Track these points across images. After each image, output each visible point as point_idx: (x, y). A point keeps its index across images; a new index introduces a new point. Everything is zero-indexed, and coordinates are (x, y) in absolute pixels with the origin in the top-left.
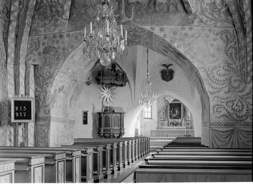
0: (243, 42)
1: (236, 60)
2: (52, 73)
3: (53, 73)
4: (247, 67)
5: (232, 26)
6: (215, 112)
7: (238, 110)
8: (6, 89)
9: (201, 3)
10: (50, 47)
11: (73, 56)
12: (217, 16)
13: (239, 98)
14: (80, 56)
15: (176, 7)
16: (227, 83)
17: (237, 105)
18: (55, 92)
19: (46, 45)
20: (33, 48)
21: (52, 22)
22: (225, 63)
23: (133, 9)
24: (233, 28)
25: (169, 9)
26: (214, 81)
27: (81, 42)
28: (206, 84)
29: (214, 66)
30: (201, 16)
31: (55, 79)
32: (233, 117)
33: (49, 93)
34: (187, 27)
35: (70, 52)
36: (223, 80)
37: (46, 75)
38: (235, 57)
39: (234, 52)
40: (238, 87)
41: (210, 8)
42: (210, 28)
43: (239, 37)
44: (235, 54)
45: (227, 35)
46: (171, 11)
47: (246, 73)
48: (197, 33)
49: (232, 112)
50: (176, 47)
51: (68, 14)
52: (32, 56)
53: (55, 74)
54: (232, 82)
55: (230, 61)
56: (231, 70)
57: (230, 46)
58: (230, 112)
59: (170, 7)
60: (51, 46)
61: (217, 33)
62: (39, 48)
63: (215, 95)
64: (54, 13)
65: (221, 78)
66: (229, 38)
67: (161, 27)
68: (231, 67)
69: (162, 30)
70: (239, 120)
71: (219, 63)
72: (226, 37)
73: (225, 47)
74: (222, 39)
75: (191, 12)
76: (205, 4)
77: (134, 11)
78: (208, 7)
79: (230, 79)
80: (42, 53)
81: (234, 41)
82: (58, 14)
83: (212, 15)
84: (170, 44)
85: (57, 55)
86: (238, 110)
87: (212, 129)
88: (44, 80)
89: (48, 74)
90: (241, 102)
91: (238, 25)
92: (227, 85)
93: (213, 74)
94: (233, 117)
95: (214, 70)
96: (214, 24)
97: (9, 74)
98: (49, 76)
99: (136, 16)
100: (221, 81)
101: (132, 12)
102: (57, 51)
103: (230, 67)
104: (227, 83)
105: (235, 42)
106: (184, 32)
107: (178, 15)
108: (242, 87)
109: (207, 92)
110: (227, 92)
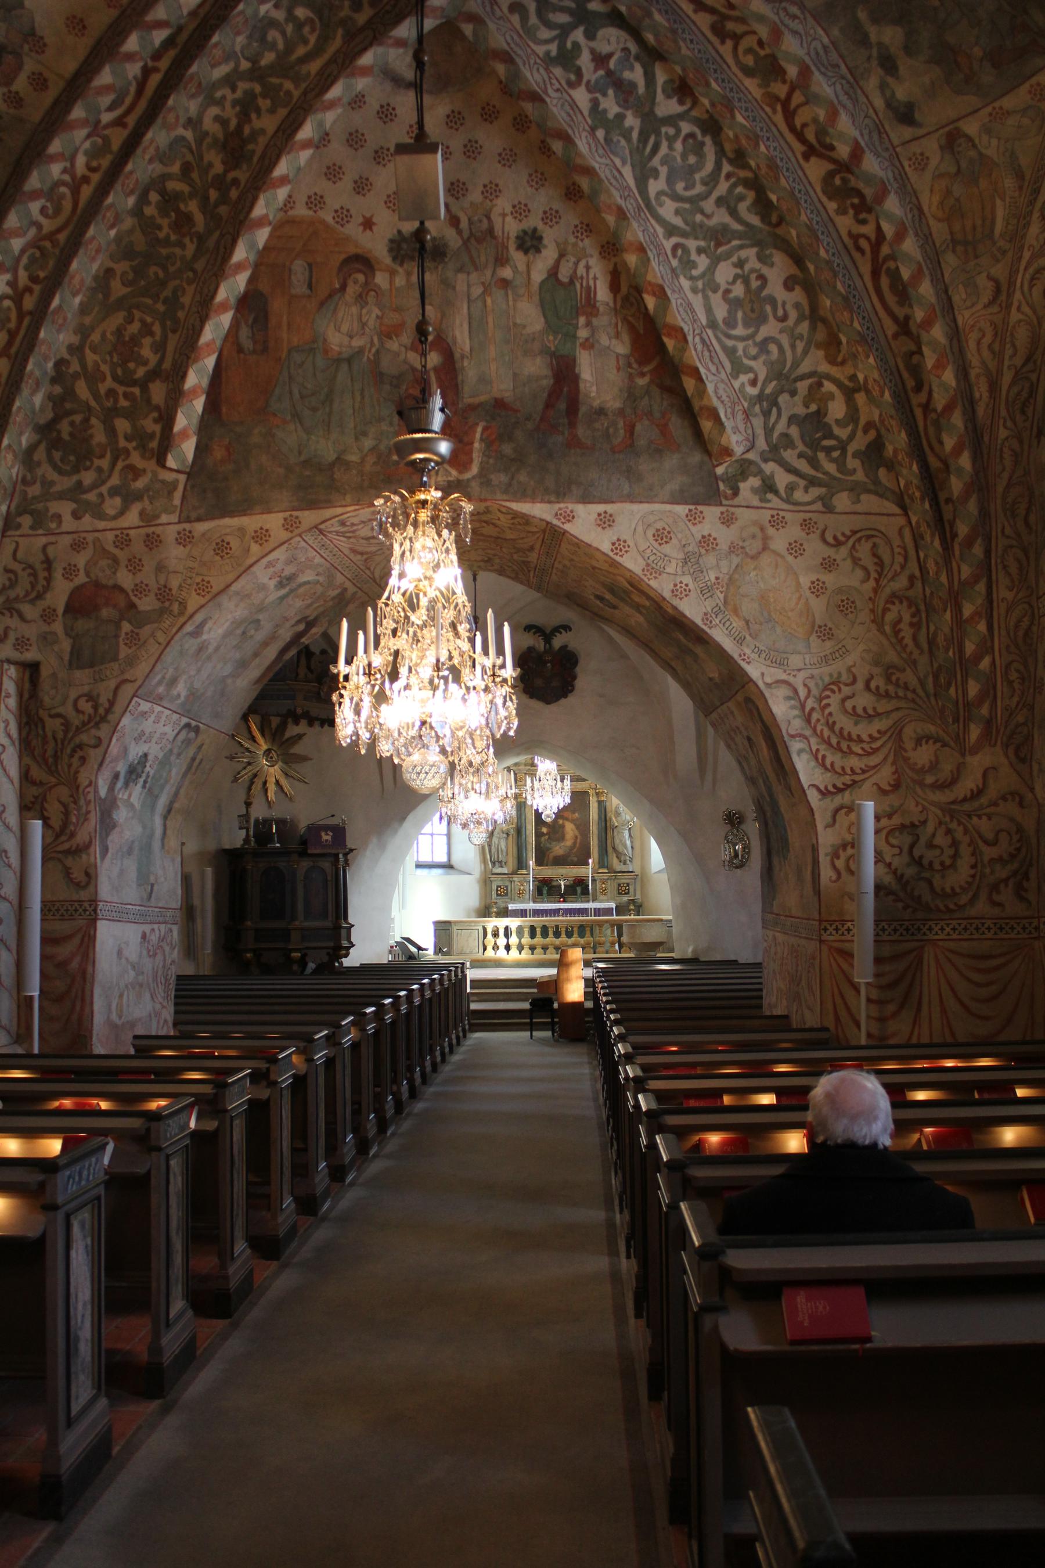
0: (944, 578)
1: (916, 652)
2: (103, 700)
3: (112, 703)
4: (965, 682)
5: (897, 510)
7: (937, 866)
9: (766, 414)
11: (202, 625)
12: (831, 468)
13: (939, 812)
15: (664, 429)
16: (885, 750)
17: (931, 846)
18: (111, 788)
19: (81, 579)
20: (19, 591)
21: (115, 480)
22: (876, 663)
23: (479, 429)
24: (901, 521)
25: (632, 434)
26: (834, 741)
27: (242, 569)
29: (831, 675)
30: (769, 467)
31: (119, 728)
32: (916, 893)
33: (91, 789)
34: (712, 512)
35: (190, 609)
36: (870, 736)
37: (78, 711)
38: (915, 639)
39: (907, 618)
40: (934, 766)
41: (802, 437)
42: (808, 516)
43: (926, 556)
44: (912, 625)
45: (875, 545)
46: (642, 442)
47: (961, 706)
48: (754, 537)
49: (911, 872)
50: (667, 595)
51: (188, 448)
52: (14, 622)
53: (118, 708)
54: (909, 745)
55: (892, 657)
56: (901, 693)
57: (894, 595)
58: (902, 875)
59: (638, 428)
60: (104, 582)
61: (835, 538)
62: (45, 592)
63: (838, 800)
64: (122, 443)
65: (861, 726)
66: (886, 558)
67: (601, 508)
68: (898, 679)
69: (605, 521)
70: (942, 908)
71: (851, 663)
72: (875, 555)
73: (870, 599)
74: (856, 561)
75: (727, 452)
76: (784, 420)
77: (482, 440)
78: (794, 431)
79: (896, 733)
80: (60, 610)
81: (907, 572)
82: (142, 447)
83: (814, 463)
85: (130, 623)
87: (830, 948)
90: (949, 832)
92: (885, 759)
93: (827, 711)
94: (916, 893)
95: (828, 693)
96: (820, 498)
98: (90, 715)
99: (491, 461)
100: (860, 740)
101: (476, 445)
102: (132, 606)
103: (894, 678)
104: (885, 750)
105: (912, 578)
107: (671, 461)
108: (947, 768)
109: (806, 786)
110: (888, 788)
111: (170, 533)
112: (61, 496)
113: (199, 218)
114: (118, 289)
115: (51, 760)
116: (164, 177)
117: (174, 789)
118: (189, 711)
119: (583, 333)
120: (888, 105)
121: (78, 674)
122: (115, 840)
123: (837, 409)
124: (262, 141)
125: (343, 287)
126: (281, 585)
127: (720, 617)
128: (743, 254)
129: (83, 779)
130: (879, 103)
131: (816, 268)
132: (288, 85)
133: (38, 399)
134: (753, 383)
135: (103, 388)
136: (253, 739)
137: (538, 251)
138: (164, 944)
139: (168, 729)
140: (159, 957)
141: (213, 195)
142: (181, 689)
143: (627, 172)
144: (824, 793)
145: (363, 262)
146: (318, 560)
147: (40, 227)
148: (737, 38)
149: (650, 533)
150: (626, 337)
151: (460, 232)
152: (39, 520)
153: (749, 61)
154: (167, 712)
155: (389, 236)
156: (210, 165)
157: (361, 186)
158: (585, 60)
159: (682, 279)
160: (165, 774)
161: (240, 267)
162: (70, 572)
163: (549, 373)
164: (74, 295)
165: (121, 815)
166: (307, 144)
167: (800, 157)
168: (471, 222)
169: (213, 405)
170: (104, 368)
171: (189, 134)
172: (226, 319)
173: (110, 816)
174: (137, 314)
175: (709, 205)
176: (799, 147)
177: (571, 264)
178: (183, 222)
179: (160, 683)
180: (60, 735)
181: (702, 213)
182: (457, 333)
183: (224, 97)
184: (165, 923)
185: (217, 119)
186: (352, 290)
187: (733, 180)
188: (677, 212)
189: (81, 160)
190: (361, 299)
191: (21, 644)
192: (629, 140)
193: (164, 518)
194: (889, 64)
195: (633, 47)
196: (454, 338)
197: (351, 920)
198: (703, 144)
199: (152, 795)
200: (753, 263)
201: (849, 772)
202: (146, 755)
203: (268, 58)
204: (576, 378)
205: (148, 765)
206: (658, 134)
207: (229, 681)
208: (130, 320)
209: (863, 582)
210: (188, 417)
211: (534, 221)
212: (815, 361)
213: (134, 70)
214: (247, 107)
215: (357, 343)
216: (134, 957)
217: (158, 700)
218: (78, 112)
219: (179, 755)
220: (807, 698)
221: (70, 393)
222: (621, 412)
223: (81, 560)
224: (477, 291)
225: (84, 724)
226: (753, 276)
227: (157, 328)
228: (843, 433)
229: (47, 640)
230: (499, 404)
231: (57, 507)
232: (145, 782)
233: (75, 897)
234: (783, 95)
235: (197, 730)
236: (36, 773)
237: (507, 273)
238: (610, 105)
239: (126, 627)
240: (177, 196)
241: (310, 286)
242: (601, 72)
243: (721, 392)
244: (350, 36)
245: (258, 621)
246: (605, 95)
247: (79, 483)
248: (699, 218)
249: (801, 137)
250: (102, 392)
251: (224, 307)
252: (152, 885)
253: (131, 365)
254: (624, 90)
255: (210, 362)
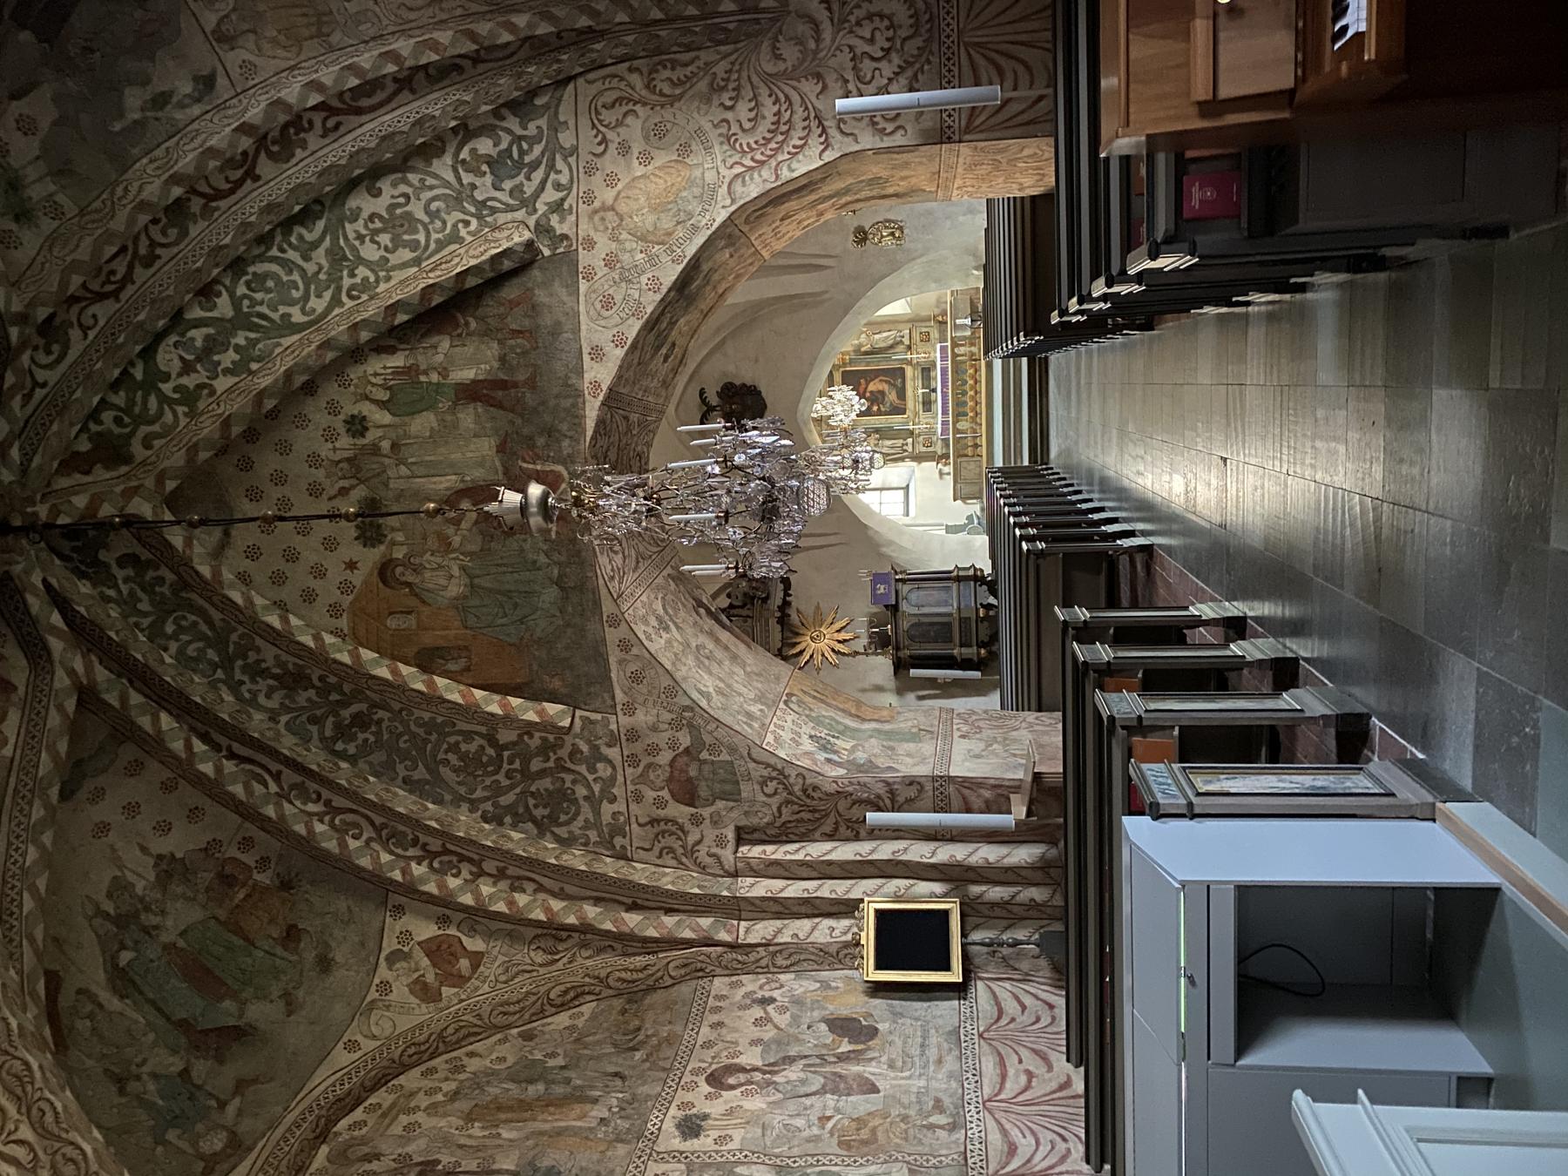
0: (630, 39)
1: (697, 63)
3: (768, 765)
5: (571, 86)
6: (899, 127)
7: (890, 34)
8: (833, 950)
9: (494, 211)
10: (670, 780)
12: (537, 150)
13: (841, 34)
15: (513, 304)
16: (787, 89)
17: (872, 41)
18: (839, 765)
19: (665, 794)
20: (677, 845)
21: (583, 769)
22: (709, 101)
23: (525, 465)
24: (581, 81)
25: (520, 332)
26: (780, 138)
27: (653, 661)
28: (793, 171)
29: (722, 143)
30: (541, 208)
32: (916, 52)
34: (584, 258)
35: (688, 702)
36: (774, 104)
37: (775, 793)
38: (686, 65)
39: (666, 73)
40: (800, 42)
41: (513, 177)
42: (581, 170)
43: (610, 57)
44: (673, 69)
45: (603, 106)
46: (527, 323)
47: (746, 17)
48: (603, 219)
49: (896, 59)
50: (658, 297)
51: (552, 708)
53: (772, 761)
54: (781, 66)
55: (702, 85)
56: (735, 76)
57: (647, 87)
58: (899, 67)
59: (514, 326)
61: (600, 144)
62: (677, 823)
63: (833, 132)
64: (551, 764)
66: (614, 95)
67: (586, 358)
68: (723, 80)
69: (598, 354)
70: (928, 26)
72: (613, 106)
74: (619, 123)
75: (530, 245)
76: (498, 194)
78: (508, 185)
79: (770, 79)
81: (626, 75)
82: (554, 747)
83: (534, 166)
84: (648, 321)
86: (890, 34)
88: (793, 803)
89: (772, 786)
90: (858, 24)
91: (567, 60)
92: (794, 88)
93: (754, 146)
94: (916, 52)
95: (737, 145)
96: (565, 159)
97: (775, 936)
100: (778, 113)
101: (539, 467)
102: (687, 750)
103: (722, 84)
104: (787, 89)
105: (630, 70)
106: (601, 271)
107: (541, 296)
109: (821, 163)
110: (820, 85)
111: (624, 720)
112: (597, 813)
113: (355, 708)
114: (420, 773)
115: (817, 815)
116: (322, 739)
118: (774, 702)
119: (435, 377)
120: (198, 100)
121: (744, 795)
122: (882, 762)
123: (485, 146)
124: (285, 657)
125: (409, 585)
126: (667, 629)
127: (675, 248)
128: (351, 235)
129: (832, 788)
130: (196, 110)
131: (357, 167)
132: (234, 637)
133: (516, 835)
134: (467, 223)
135: (505, 782)
136: (801, 652)
137: (364, 418)
138: (970, 720)
139: (789, 719)
140: (981, 724)
141: (334, 697)
142: (755, 709)
143: (286, 341)
144: (827, 145)
145: (385, 571)
146: (644, 598)
147: (370, 840)
148: (153, 244)
149: (607, 314)
150: (435, 339)
151: (353, 487)
152: (617, 830)
153: (173, 233)
154: (775, 719)
155: (361, 547)
156: (309, 700)
157: (319, 572)
158: (189, 381)
159: (378, 290)
161: (395, 672)
162: (660, 803)
163: (472, 405)
164: (427, 809)
165: (861, 756)
166: (285, 620)
167: (258, 184)
168: (345, 478)
169: (516, 691)
170: (488, 782)
171: (284, 719)
172: (441, 682)
173: (863, 765)
174: (441, 756)
175: (310, 268)
176: (249, 184)
177: (374, 390)
178: (360, 721)
179: (750, 726)
180: (796, 808)
181: (318, 273)
182: (442, 486)
183: (249, 691)
185: (268, 696)
186: (410, 578)
187: (285, 246)
188: (319, 296)
189: (311, 807)
190: (417, 570)
191: (721, 842)
192: (258, 341)
193: (613, 727)
194: (161, 100)
195: (173, 339)
196: (447, 489)
197: (952, 568)
198: (255, 274)
199: (845, 732)
200: (359, 226)
201: (807, 123)
202: (811, 737)
203: (211, 654)
204: (474, 382)
206: (250, 315)
207: (748, 669)
208: (446, 762)
209: (637, 116)
210: (526, 710)
211: (338, 423)
212: (443, 167)
213: (229, 766)
214: (257, 672)
215: (456, 571)
216: (982, 745)
218: (270, 811)
219: (811, 710)
220: (743, 165)
221: (510, 809)
222: (500, 342)
223: (650, 794)
224: (403, 470)
225: (786, 788)
226: (371, 226)
227: (452, 739)
228: (506, 141)
229: (716, 822)
230: (501, 449)
231: (606, 818)
232: (833, 737)
233: (931, 793)
234: (203, 201)
235: (790, 695)
236: (828, 828)
237: (385, 445)
238: (229, 358)
239: (704, 755)
240: (338, 726)
241: (409, 613)
242: (199, 367)
243: (476, 253)
244: (186, 586)
246: (219, 363)
247: (586, 798)
248: (322, 276)
249: (239, 183)
250: (508, 782)
251: (431, 684)
253: (485, 759)
254: (213, 346)
255: (479, 694)
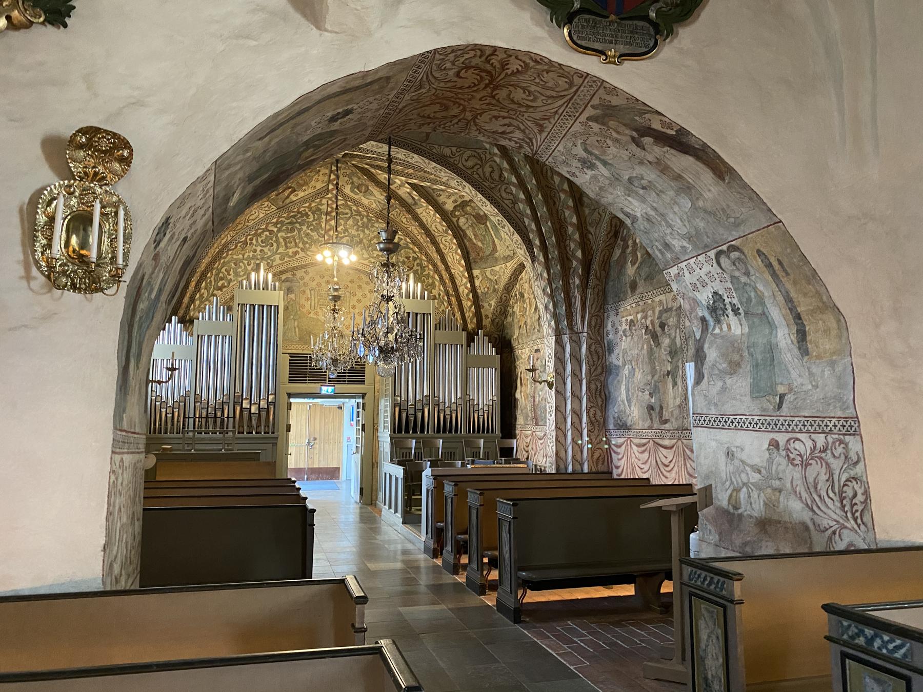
14: (629, 198)
117: (780, 298)
138: (828, 456)
139: (707, 268)
142: (677, 243)
146: (560, 148)
160: (752, 294)
184: (823, 432)
202: (715, 293)
205: (725, 298)
207: (700, 203)
217: (677, 260)
232: (736, 311)
245: (630, 180)
252: (782, 397)
